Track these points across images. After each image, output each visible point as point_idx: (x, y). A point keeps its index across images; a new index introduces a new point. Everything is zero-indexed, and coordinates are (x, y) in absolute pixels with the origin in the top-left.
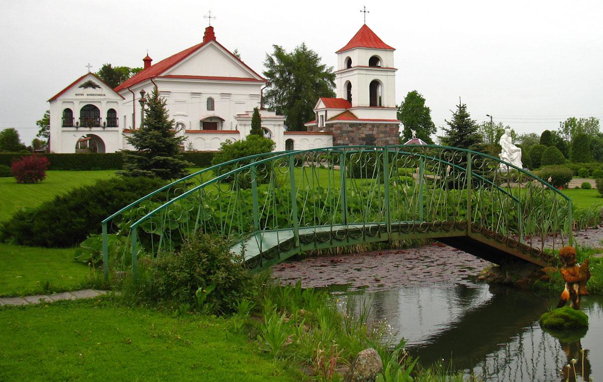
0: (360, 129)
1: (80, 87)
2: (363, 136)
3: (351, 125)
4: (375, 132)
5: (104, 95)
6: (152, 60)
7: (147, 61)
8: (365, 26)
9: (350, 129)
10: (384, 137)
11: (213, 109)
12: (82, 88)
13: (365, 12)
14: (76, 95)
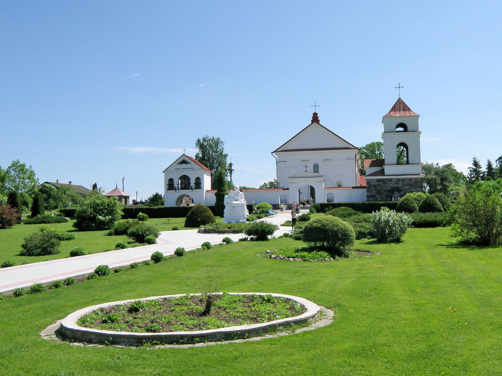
0: (386, 183)
1: (178, 164)
2: (389, 188)
3: (378, 180)
4: (400, 185)
5: (193, 168)
8: (399, 99)
9: (376, 183)
10: (409, 189)
11: (318, 172)
14: (176, 169)
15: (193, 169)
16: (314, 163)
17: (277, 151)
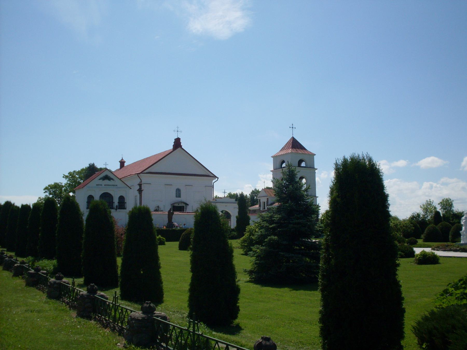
1: (100, 179)
5: (116, 185)
6: (125, 162)
7: (122, 163)
11: (180, 197)
12: (101, 180)
13: (293, 128)
15: (101, 186)
16: (176, 188)
17: (145, 172)
